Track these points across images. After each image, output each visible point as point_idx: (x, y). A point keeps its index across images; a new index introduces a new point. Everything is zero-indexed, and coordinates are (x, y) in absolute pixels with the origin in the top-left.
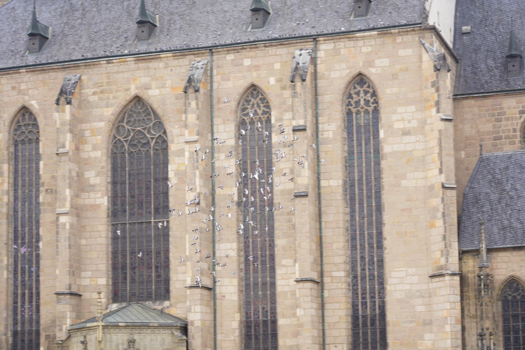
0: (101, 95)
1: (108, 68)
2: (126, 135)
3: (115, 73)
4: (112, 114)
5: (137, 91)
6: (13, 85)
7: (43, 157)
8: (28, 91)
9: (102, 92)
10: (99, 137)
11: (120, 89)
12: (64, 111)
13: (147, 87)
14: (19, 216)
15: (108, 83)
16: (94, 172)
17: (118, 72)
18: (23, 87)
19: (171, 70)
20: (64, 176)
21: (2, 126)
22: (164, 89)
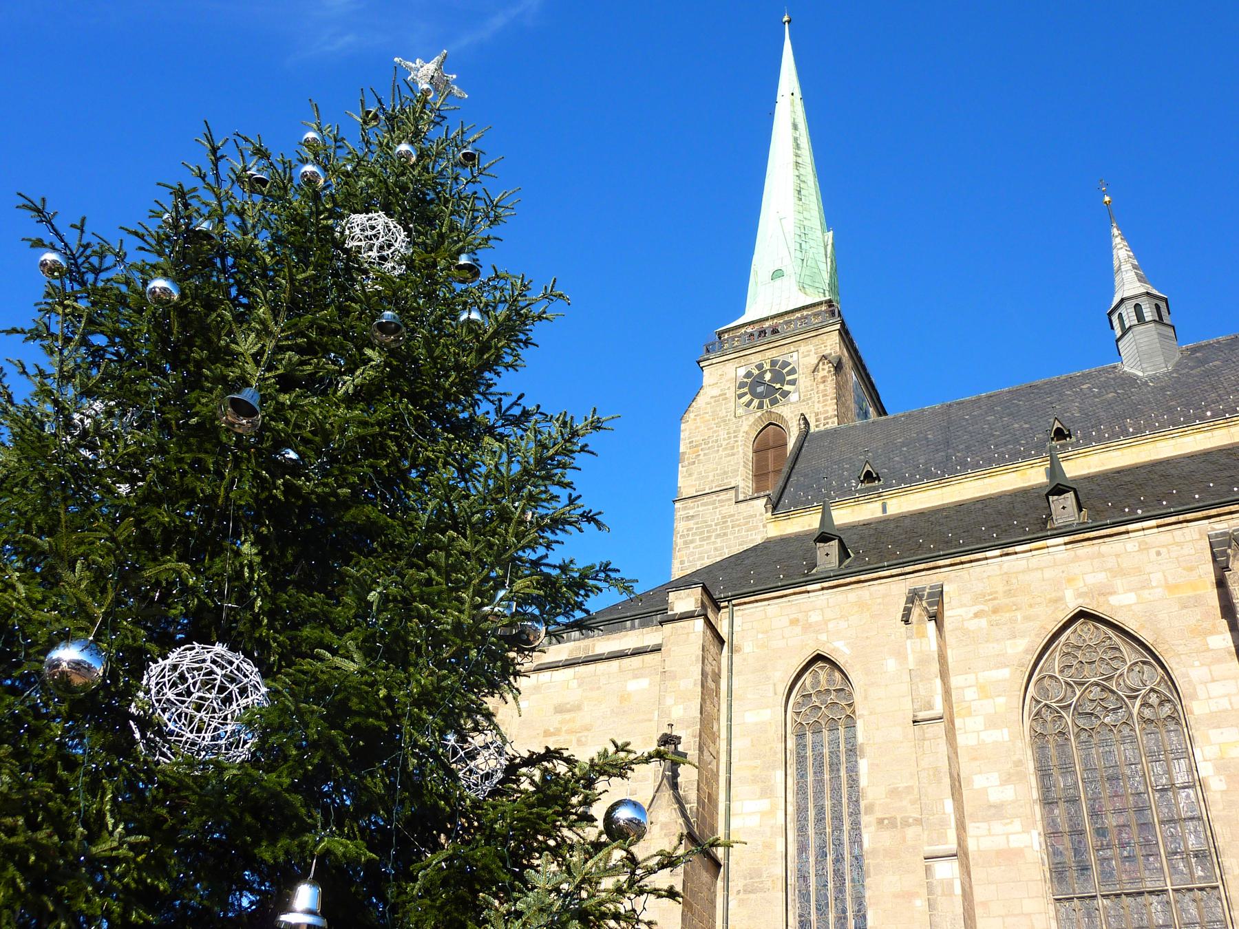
0: (994, 617)
1: (1005, 566)
2: (1062, 695)
3: (1024, 572)
4: (1026, 651)
5: (1080, 601)
6: (792, 617)
7: (867, 750)
8: (826, 624)
9: (995, 611)
10: (1001, 701)
11: (1039, 600)
12: (923, 635)
13: (1105, 592)
14: (812, 889)
15: (1008, 593)
16: (996, 775)
17: (1029, 570)
18: (815, 617)
19: (1158, 553)
20: (937, 770)
21: (771, 693)
22: (1146, 592)
